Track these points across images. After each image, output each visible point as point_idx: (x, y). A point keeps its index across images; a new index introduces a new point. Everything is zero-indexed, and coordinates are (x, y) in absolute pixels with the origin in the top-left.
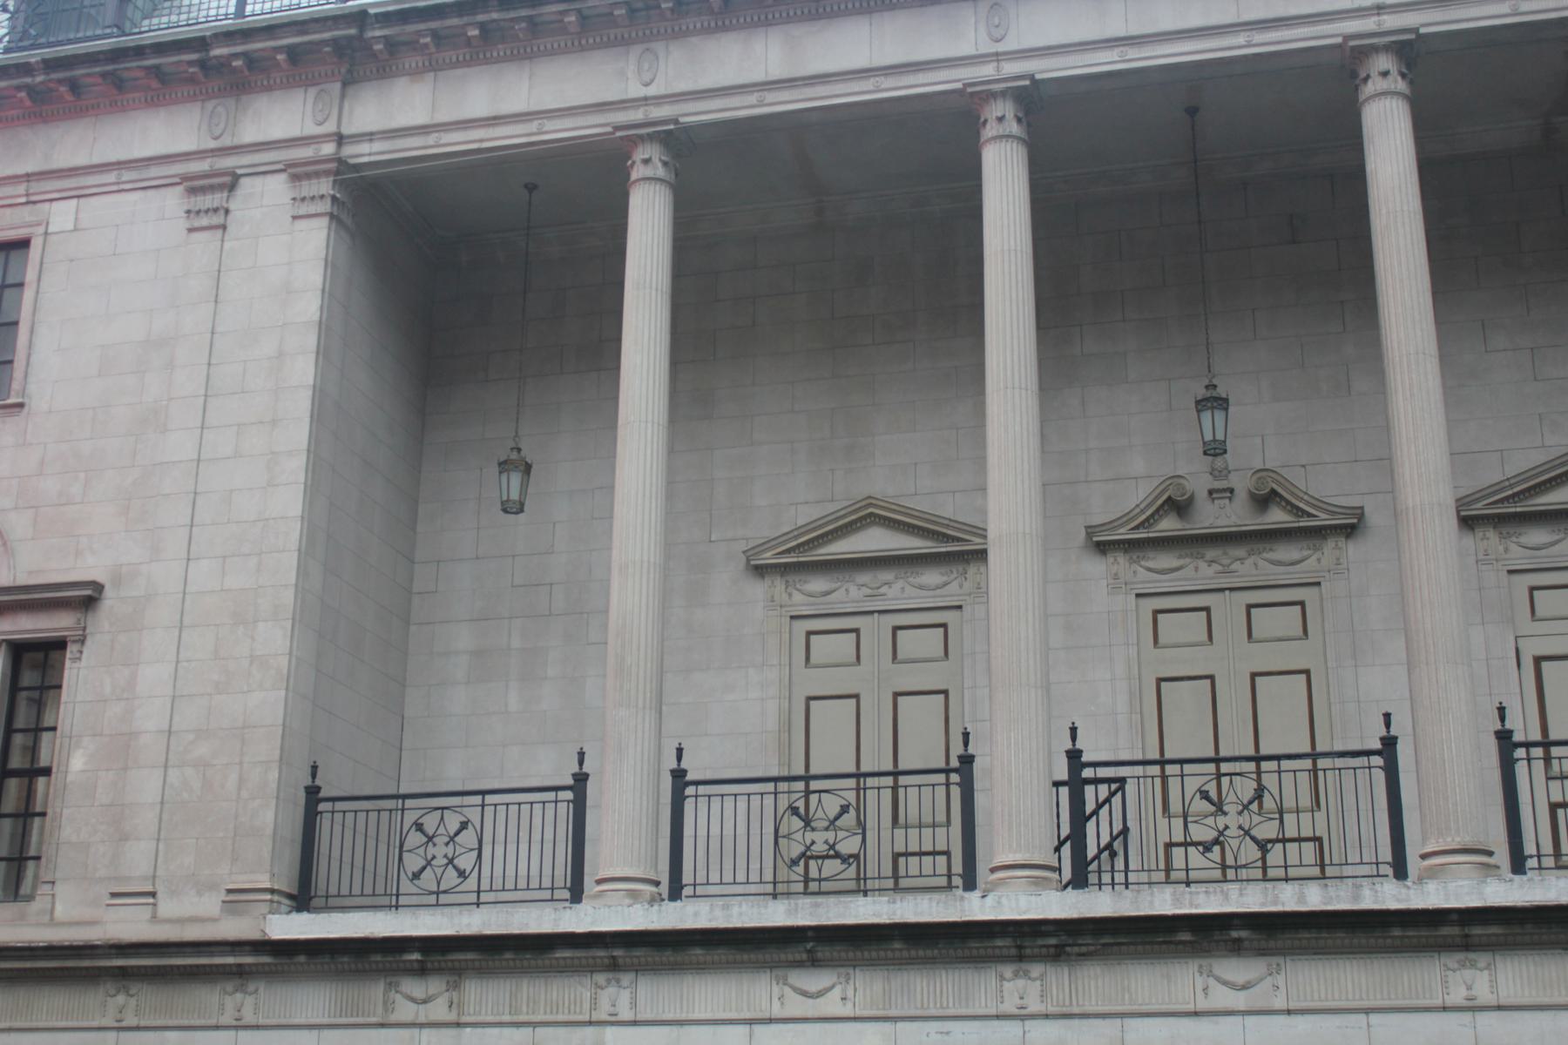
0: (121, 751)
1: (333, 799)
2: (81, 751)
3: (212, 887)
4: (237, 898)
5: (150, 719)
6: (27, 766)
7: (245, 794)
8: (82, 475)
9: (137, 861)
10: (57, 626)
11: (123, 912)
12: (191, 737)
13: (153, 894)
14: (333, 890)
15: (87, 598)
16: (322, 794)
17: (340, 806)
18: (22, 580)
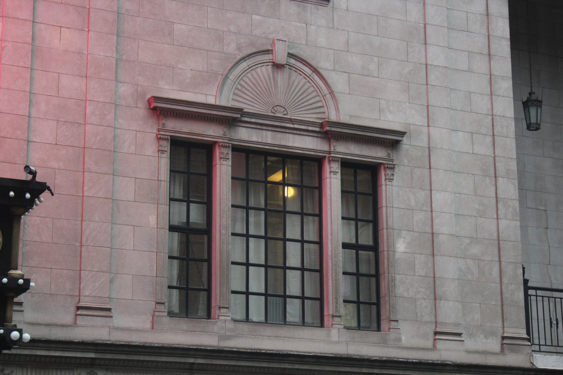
0: (431, 242)
1: (536, 289)
2: (402, 239)
3: (493, 334)
4: (508, 342)
5: (444, 226)
6: (354, 241)
7: (505, 280)
8: (376, 59)
9: (450, 313)
10: (374, 155)
11: (448, 345)
12: (468, 241)
13: (459, 335)
14: (542, 342)
15: (391, 140)
16: (530, 284)
17: (539, 293)
18: (344, 119)
